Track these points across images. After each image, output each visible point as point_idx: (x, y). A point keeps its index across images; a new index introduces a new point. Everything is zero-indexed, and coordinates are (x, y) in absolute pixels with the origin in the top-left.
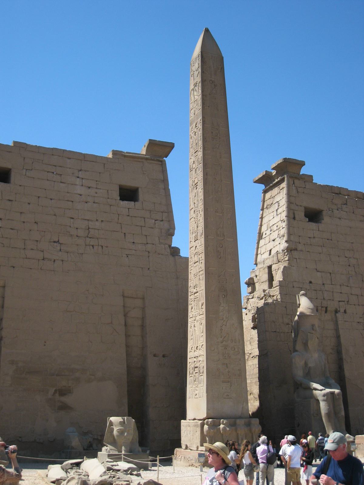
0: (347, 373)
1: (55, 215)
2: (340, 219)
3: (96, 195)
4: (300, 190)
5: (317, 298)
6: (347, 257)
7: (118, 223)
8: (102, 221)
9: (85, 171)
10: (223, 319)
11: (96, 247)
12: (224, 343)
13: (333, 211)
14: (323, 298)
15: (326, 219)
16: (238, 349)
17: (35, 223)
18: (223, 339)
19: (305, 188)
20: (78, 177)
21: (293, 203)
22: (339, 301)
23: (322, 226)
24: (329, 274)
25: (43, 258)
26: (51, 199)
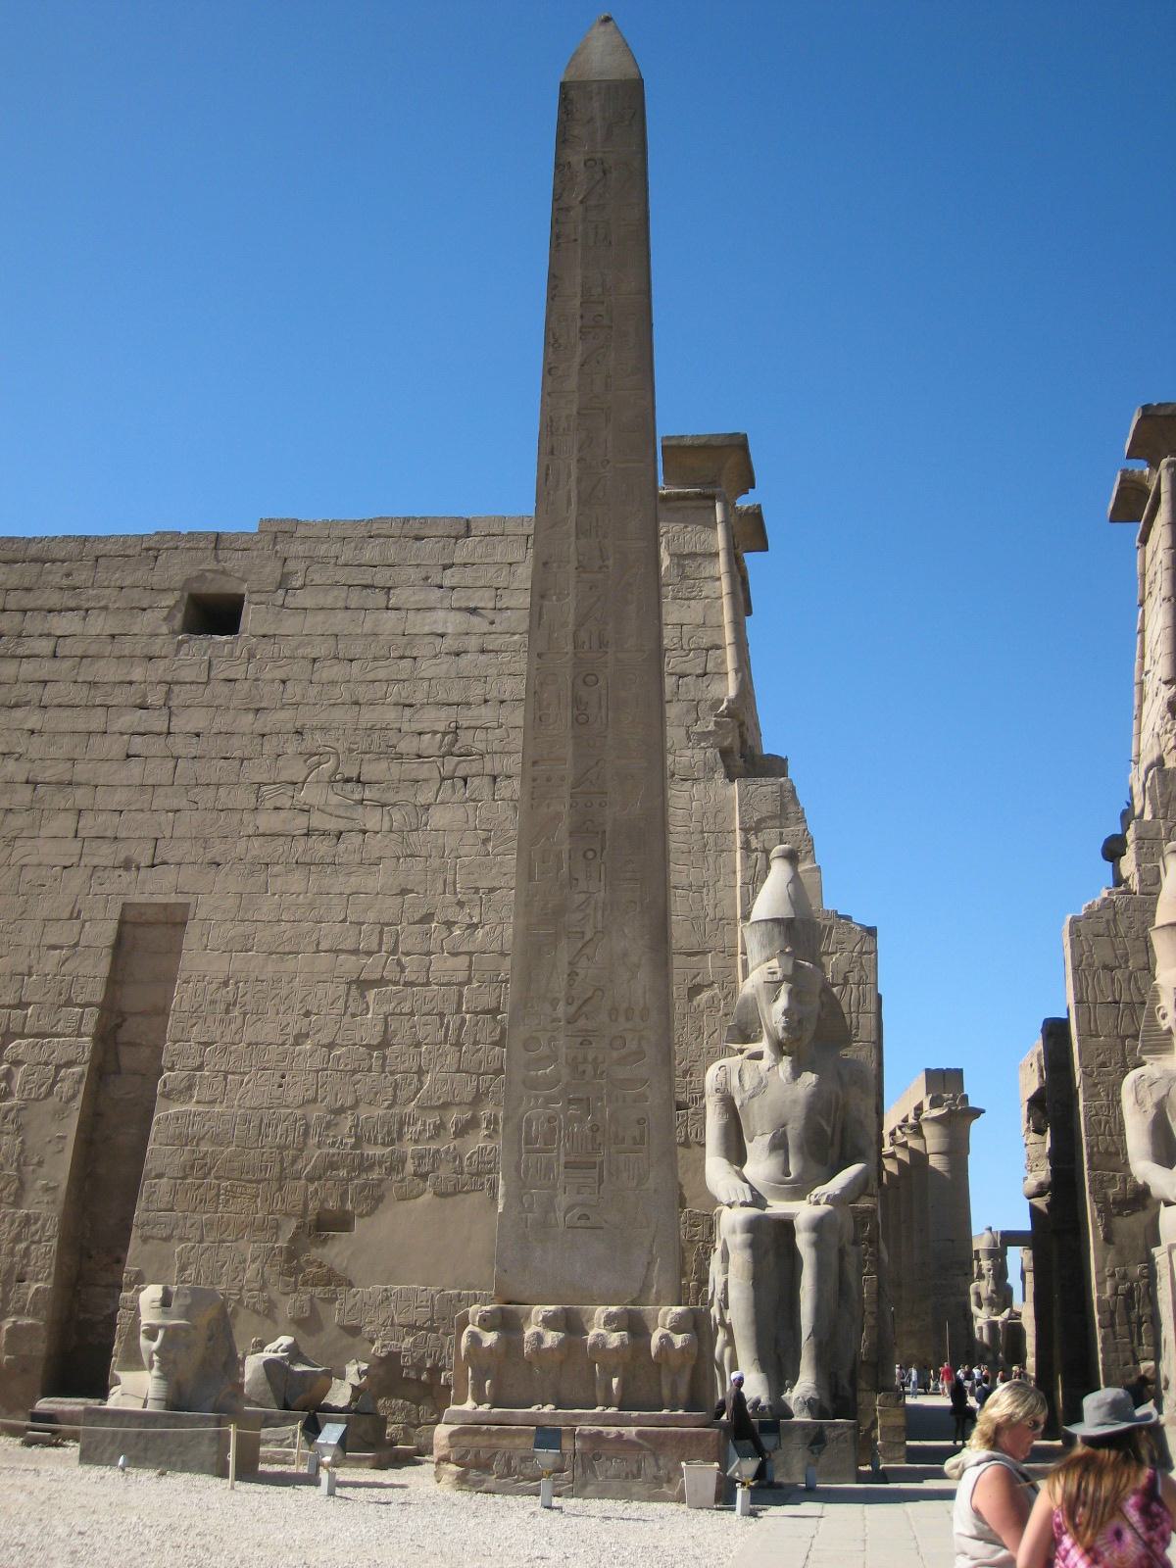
1: (356, 703)
3: (493, 628)
8: (502, 702)
10: (583, 937)
11: (474, 782)
12: (582, 1023)
16: (640, 1044)
17: (297, 732)
18: (580, 1008)
25: (305, 831)
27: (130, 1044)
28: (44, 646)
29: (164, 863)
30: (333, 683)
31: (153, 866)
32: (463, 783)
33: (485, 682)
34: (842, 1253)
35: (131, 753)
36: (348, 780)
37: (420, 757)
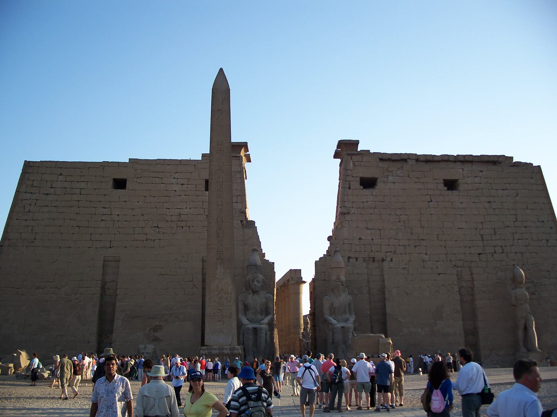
0: (388, 310)
1: (156, 208)
2: (394, 183)
3: (188, 189)
4: (356, 164)
5: (365, 251)
6: (398, 215)
7: (202, 208)
8: (190, 208)
9: (180, 173)
13: (387, 178)
14: (371, 251)
15: (380, 185)
18: (219, 292)
19: (362, 161)
20: (174, 178)
21: (349, 176)
22: (386, 252)
23: (375, 191)
24: (379, 230)
25: (146, 239)
26: (154, 197)
27: (108, 289)
28: (77, 191)
29: (113, 247)
30: (150, 202)
31: (110, 247)
32: (182, 228)
33: (186, 203)
34: (266, 334)
35: (102, 219)
36: (155, 227)
37: (171, 221)
